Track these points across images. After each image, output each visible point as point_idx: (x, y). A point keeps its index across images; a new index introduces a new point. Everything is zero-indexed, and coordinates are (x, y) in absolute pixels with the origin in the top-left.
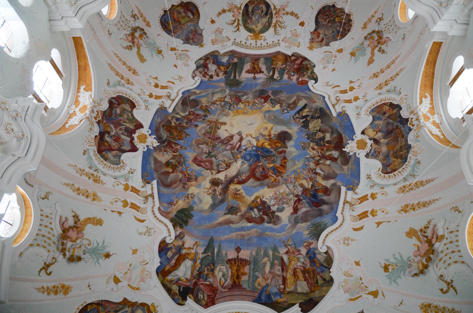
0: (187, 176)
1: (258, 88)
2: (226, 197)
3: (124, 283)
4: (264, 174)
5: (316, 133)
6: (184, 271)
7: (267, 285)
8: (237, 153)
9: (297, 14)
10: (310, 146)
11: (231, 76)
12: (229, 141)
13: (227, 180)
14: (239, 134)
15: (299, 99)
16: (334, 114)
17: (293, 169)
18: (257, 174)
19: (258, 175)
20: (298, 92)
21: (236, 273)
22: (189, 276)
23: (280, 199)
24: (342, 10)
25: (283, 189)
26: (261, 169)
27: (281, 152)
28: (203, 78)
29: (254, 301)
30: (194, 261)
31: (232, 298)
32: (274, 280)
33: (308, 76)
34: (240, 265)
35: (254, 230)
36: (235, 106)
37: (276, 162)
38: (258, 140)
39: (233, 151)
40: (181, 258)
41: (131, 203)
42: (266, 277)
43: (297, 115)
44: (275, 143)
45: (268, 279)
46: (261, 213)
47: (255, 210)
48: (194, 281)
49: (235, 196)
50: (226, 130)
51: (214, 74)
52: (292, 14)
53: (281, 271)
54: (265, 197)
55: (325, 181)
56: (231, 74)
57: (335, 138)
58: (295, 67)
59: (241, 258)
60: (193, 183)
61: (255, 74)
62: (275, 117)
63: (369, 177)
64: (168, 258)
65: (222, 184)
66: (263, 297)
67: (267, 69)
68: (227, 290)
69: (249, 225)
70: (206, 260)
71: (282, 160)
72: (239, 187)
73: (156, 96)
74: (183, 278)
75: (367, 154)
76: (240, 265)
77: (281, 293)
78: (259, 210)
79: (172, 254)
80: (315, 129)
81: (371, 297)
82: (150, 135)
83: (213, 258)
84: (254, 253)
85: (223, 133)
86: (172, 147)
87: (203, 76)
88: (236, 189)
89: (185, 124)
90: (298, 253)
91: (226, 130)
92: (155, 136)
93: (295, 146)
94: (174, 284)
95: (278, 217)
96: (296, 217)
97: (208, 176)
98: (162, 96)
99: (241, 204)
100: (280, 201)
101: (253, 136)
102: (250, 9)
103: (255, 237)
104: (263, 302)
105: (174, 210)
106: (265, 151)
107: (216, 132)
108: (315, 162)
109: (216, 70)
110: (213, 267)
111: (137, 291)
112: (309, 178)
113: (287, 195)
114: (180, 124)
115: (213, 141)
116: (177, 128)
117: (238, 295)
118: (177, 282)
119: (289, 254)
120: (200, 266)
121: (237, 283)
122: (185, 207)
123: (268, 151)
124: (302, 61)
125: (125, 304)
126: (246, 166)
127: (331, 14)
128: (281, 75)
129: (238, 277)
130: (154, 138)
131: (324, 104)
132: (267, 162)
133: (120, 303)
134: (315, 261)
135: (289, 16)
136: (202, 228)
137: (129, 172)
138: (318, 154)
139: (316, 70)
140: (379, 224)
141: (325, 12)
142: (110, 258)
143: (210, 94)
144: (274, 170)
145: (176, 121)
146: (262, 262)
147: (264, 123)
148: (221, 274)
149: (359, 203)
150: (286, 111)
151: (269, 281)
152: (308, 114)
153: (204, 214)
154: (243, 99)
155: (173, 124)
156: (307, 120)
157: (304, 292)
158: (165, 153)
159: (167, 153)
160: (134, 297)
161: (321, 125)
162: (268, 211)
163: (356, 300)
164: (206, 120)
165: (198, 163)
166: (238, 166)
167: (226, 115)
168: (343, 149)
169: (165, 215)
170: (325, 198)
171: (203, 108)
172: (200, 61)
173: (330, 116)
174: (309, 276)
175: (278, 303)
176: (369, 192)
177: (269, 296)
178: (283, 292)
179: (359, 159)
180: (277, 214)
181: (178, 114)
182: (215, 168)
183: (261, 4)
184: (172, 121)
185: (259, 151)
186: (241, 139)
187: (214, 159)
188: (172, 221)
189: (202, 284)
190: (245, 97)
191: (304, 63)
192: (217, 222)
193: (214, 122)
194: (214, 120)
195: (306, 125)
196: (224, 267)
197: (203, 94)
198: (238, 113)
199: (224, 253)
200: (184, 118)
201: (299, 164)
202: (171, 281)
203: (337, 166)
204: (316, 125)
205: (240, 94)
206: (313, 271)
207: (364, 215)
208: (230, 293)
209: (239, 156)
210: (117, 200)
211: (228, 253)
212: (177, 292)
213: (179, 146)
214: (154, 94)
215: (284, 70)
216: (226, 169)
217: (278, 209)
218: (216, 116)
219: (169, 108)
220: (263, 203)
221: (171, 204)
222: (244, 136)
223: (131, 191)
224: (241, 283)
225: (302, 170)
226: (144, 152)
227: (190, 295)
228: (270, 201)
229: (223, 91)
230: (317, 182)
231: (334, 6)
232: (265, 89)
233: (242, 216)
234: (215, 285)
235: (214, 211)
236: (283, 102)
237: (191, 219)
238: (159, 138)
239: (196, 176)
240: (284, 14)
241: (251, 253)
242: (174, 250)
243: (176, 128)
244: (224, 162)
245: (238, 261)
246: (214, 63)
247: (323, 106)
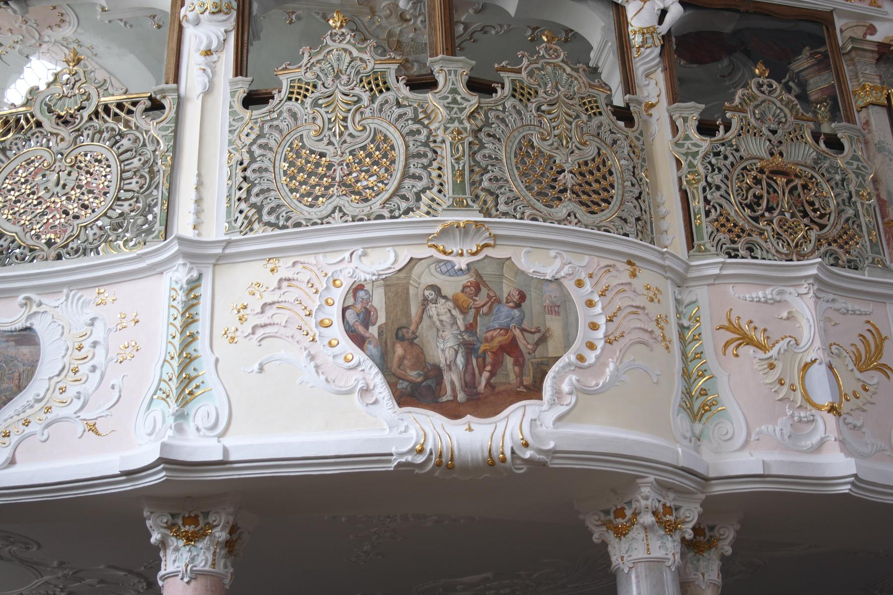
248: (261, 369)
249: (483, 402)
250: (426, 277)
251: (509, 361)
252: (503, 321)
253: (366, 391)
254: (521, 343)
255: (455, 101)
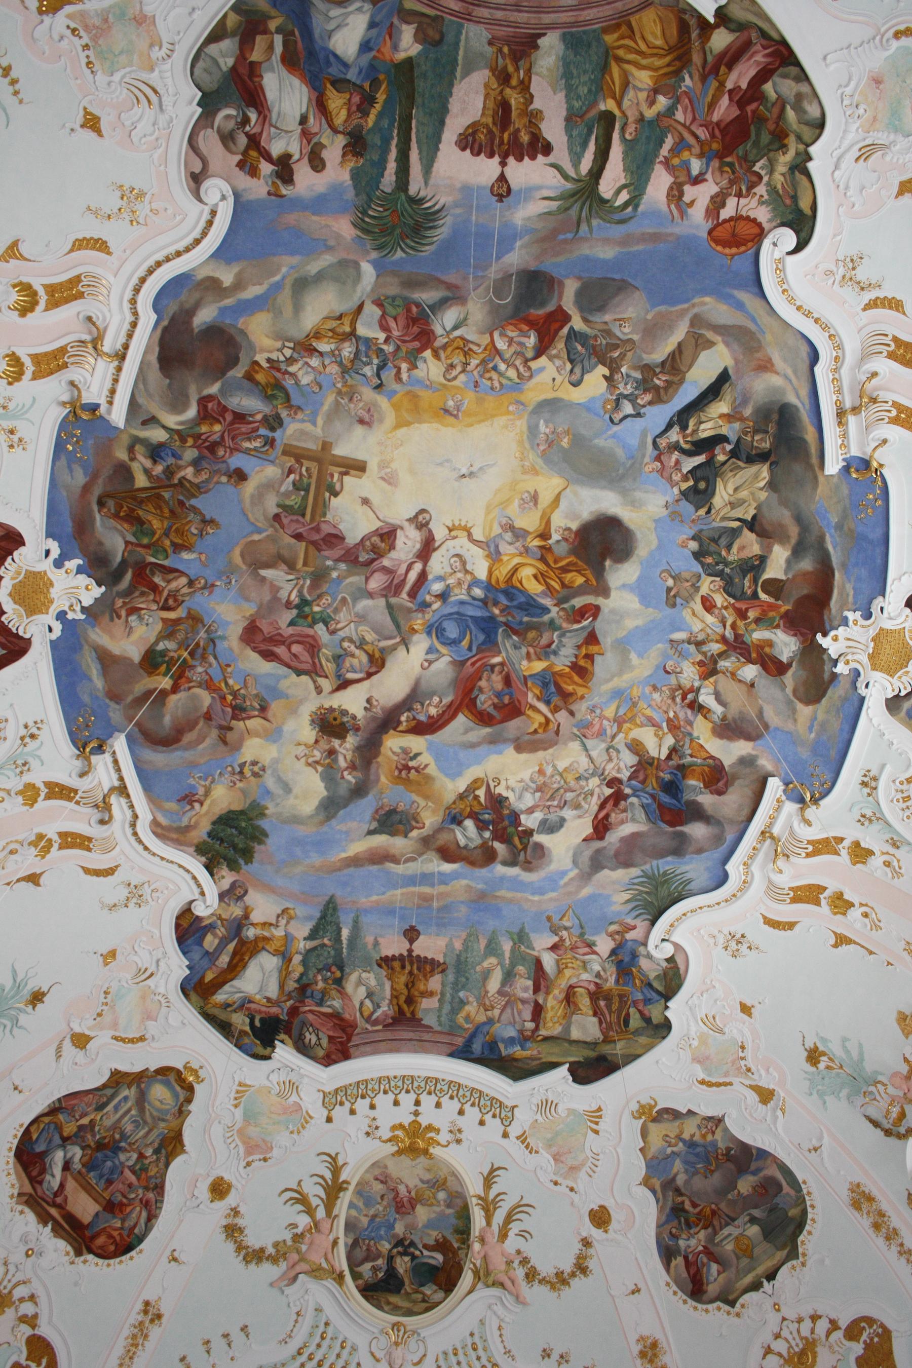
0: (229, 698)
1: (516, 258)
2: (372, 777)
3: (102, 1040)
4: (506, 700)
5: (734, 533)
6: (259, 980)
7: (490, 1021)
8: (410, 611)
10: (697, 589)
11: (381, 165)
12: (379, 554)
13: (374, 718)
14: (421, 521)
15: (697, 342)
16: (833, 466)
17: (616, 683)
18: (482, 697)
19: (485, 701)
20: (704, 292)
21: (406, 992)
22: (273, 991)
23: (549, 792)
25: (570, 756)
26: (497, 680)
27: (580, 614)
28: (244, 181)
29: (451, 1055)
30: (284, 957)
31: (395, 1046)
32: (509, 1010)
33: (772, 190)
34: (415, 971)
35: (461, 880)
36: (404, 366)
37: (555, 653)
38: (495, 556)
39: (393, 600)
40: (244, 952)
41: (60, 834)
42: (487, 1003)
43: (674, 435)
44: (565, 570)
45: (493, 1008)
46: (487, 834)
47: (469, 823)
48: (290, 1003)
49: (404, 773)
50: (365, 501)
51: (294, 148)
53: (531, 992)
54: (503, 783)
55: (719, 742)
56: (387, 142)
57: (805, 574)
58: (715, 117)
59: (418, 956)
60: (254, 723)
61: (503, 164)
62: (578, 441)
63: (869, 783)
64: (207, 952)
65: (357, 729)
66: (477, 1047)
67: (570, 120)
68: (380, 1027)
69: (447, 867)
70: (318, 956)
71: (579, 647)
72: (416, 743)
73: (35, 358)
74: (258, 997)
75: (897, 696)
76: (415, 971)
77: (524, 1039)
78: (481, 826)
79: (217, 941)
80: (738, 513)
81: (753, 1097)
82: (58, 564)
83: (339, 952)
84: (458, 945)
85: (352, 513)
86: (155, 588)
87: (241, 165)
88: (405, 751)
89: (189, 472)
90: (587, 950)
91: (365, 501)
92: (81, 562)
93: (641, 589)
94: (235, 1011)
95: (539, 847)
96: (598, 852)
97: (303, 701)
98: (63, 350)
99: (422, 803)
100: (552, 798)
101: (478, 535)
103: (462, 902)
104: (473, 1056)
105: (202, 818)
106: (520, 607)
107: (325, 506)
108: (701, 664)
109: (303, 120)
110: (338, 974)
111: (140, 1044)
112: (669, 720)
113: (578, 779)
114: (169, 472)
115: (311, 548)
116: (159, 497)
117: (410, 1040)
118: (242, 1007)
119: (560, 952)
120: (301, 969)
121: (408, 1015)
122: (236, 807)
123: (531, 606)
124: (764, 75)
125: (118, 1083)
126: (443, 665)
128: (637, 181)
129: (410, 1001)
130: (80, 570)
131: (804, 392)
132: (524, 650)
133: (104, 1086)
134: (631, 973)
136: (298, 869)
137: (22, 738)
138: (720, 630)
139: (822, 155)
140: (841, 940)
142: (45, 999)
143: (287, 292)
144: (545, 685)
145: (148, 463)
146: (478, 968)
147: (525, 472)
148: (362, 992)
149: (808, 855)
150: (628, 408)
151: (496, 1012)
152: (724, 431)
153: (302, 831)
154: (439, 330)
155: (141, 481)
156: (710, 462)
157: (588, 1040)
158: (133, 618)
159: (141, 618)
160: (134, 1061)
161: (763, 495)
162: (511, 830)
163: (714, 1088)
164: (279, 448)
165: (263, 647)
166: (416, 665)
167: (361, 422)
168: (819, 636)
169: (174, 836)
170: (706, 799)
171: (260, 377)
172: (213, 49)
173: (814, 460)
174: (609, 1006)
175: (516, 1060)
176: (852, 833)
177: (492, 1045)
178: (532, 1036)
179: (862, 699)
180: (537, 838)
181: (151, 421)
182: (329, 667)
184: (136, 467)
185: (496, 603)
186: (427, 549)
187: (320, 629)
188: (201, 850)
189: (310, 1011)
190: (450, 316)
191: (768, 88)
192: (344, 855)
193: (309, 458)
194: (311, 445)
195: (699, 492)
196: (372, 975)
197: (252, 292)
198: (414, 410)
199: (370, 939)
200: (183, 440)
201: (642, 666)
202: (226, 1006)
203: (778, 694)
204: (744, 494)
205: (427, 296)
206: (621, 996)
207: (808, 894)
208: (389, 1035)
209: (418, 622)
210: (13, 846)
211: (380, 940)
212: (247, 1029)
213: (183, 580)
214: (23, 353)
215: (653, 130)
216: (369, 675)
217: (544, 822)
218: (320, 421)
219: (110, 403)
220: (497, 802)
221: (189, 799)
222: (439, 533)
223: (48, 797)
224: (420, 1015)
225: (648, 690)
226: (54, 645)
227: (282, 1036)
228: (520, 797)
229: (346, 271)
230: (692, 740)
232: (551, 265)
233: (426, 842)
234: (347, 1016)
235: (334, 822)
236: (622, 356)
237: (261, 842)
238: (98, 566)
239: (263, 700)
241: (449, 946)
242: (221, 931)
243: (153, 496)
244: (361, 644)
245: (412, 964)
246: (290, 61)
247: (796, 398)
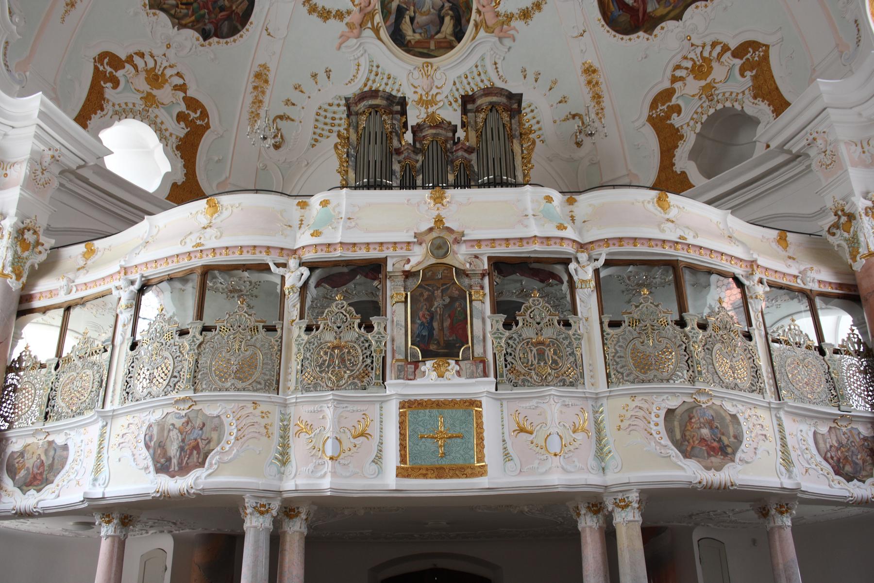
9: (310, 12)
24: (179, 22)
52: (325, 15)
102: (448, 25)
127: (209, 14)
135: (333, 6)
141: (228, 18)
183: (418, 42)
231: (206, 36)
240: (349, 13)
248: (120, 460)
249: (184, 469)
250: (171, 420)
251: (195, 452)
252: (195, 436)
253: (147, 468)
254: (200, 445)
255: (193, 341)
